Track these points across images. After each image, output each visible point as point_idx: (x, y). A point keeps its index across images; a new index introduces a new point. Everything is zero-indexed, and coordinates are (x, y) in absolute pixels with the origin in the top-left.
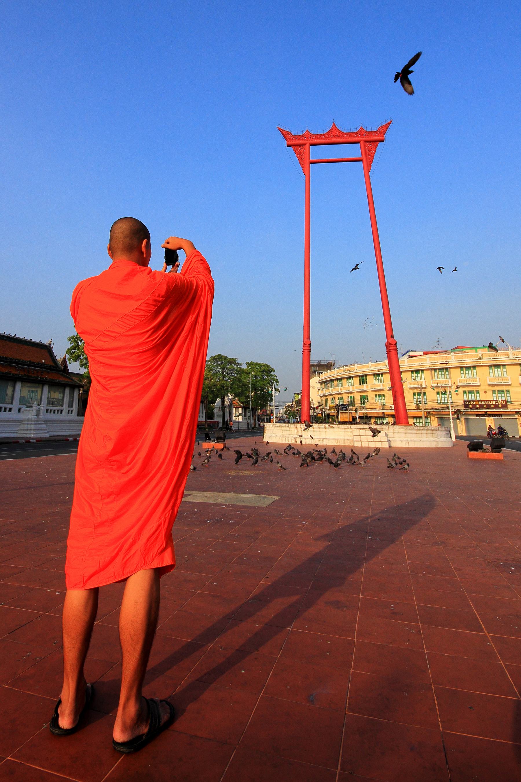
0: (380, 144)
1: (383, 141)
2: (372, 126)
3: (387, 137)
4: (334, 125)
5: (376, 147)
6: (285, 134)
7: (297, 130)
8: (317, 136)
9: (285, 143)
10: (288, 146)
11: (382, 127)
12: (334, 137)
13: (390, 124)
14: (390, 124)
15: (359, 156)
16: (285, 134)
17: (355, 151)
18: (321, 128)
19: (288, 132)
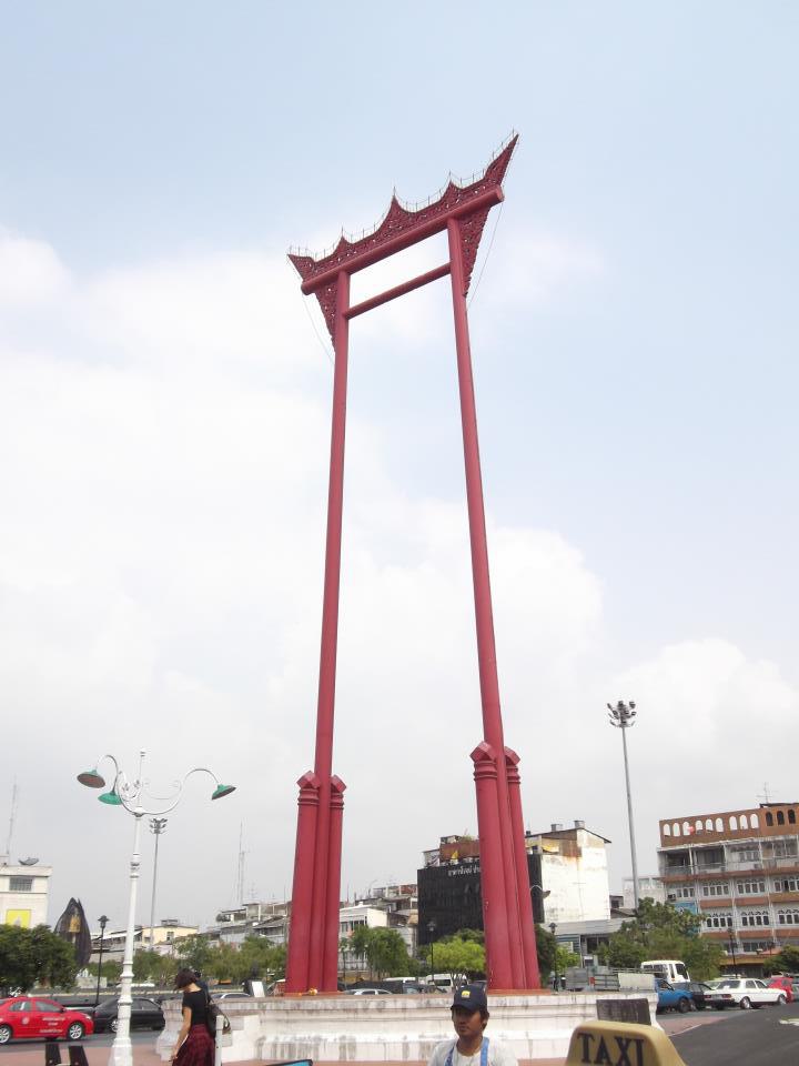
0: (494, 211)
1: (496, 200)
2: (470, 173)
3: (508, 184)
4: (395, 203)
6: (302, 264)
7: (321, 249)
8: (366, 242)
10: (306, 290)
13: (513, 144)
14: (513, 144)
16: (302, 264)
17: (434, 250)
18: (364, 223)
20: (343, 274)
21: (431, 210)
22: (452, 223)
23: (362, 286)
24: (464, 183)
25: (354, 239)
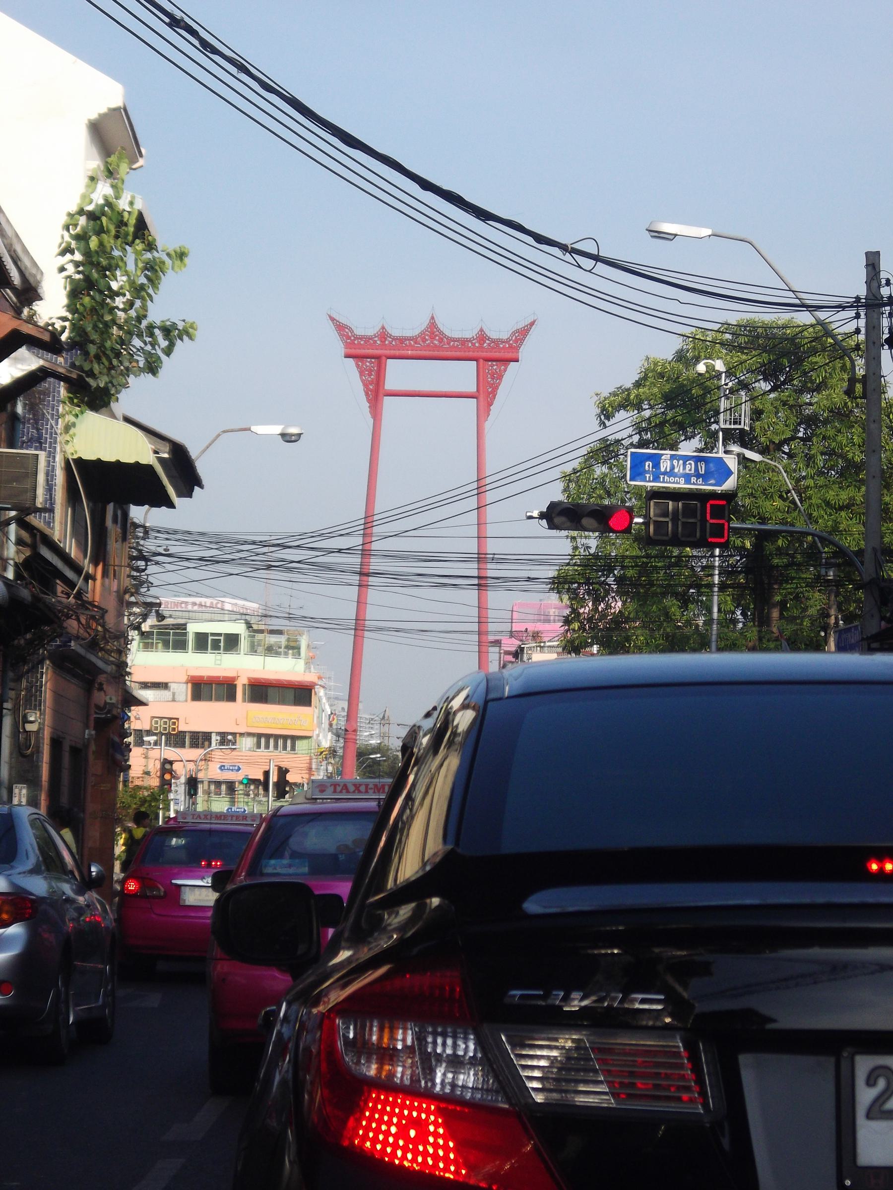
1: (517, 361)
2: (500, 330)
3: (523, 353)
5: (505, 370)
6: (341, 328)
7: (365, 326)
8: (401, 340)
9: (339, 348)
10: (347, 356)
11: (518, 331)
12: (433, 346)
13: (532, 324)
14: (532, 324)
15: (473, 388)
16: (341, 328)
19: (346, 327)
20: (384, 358)
21: (464, 341)
22: (481, 361)
23: (398, 374)
24: (494, 333)
25: (396, 331)
